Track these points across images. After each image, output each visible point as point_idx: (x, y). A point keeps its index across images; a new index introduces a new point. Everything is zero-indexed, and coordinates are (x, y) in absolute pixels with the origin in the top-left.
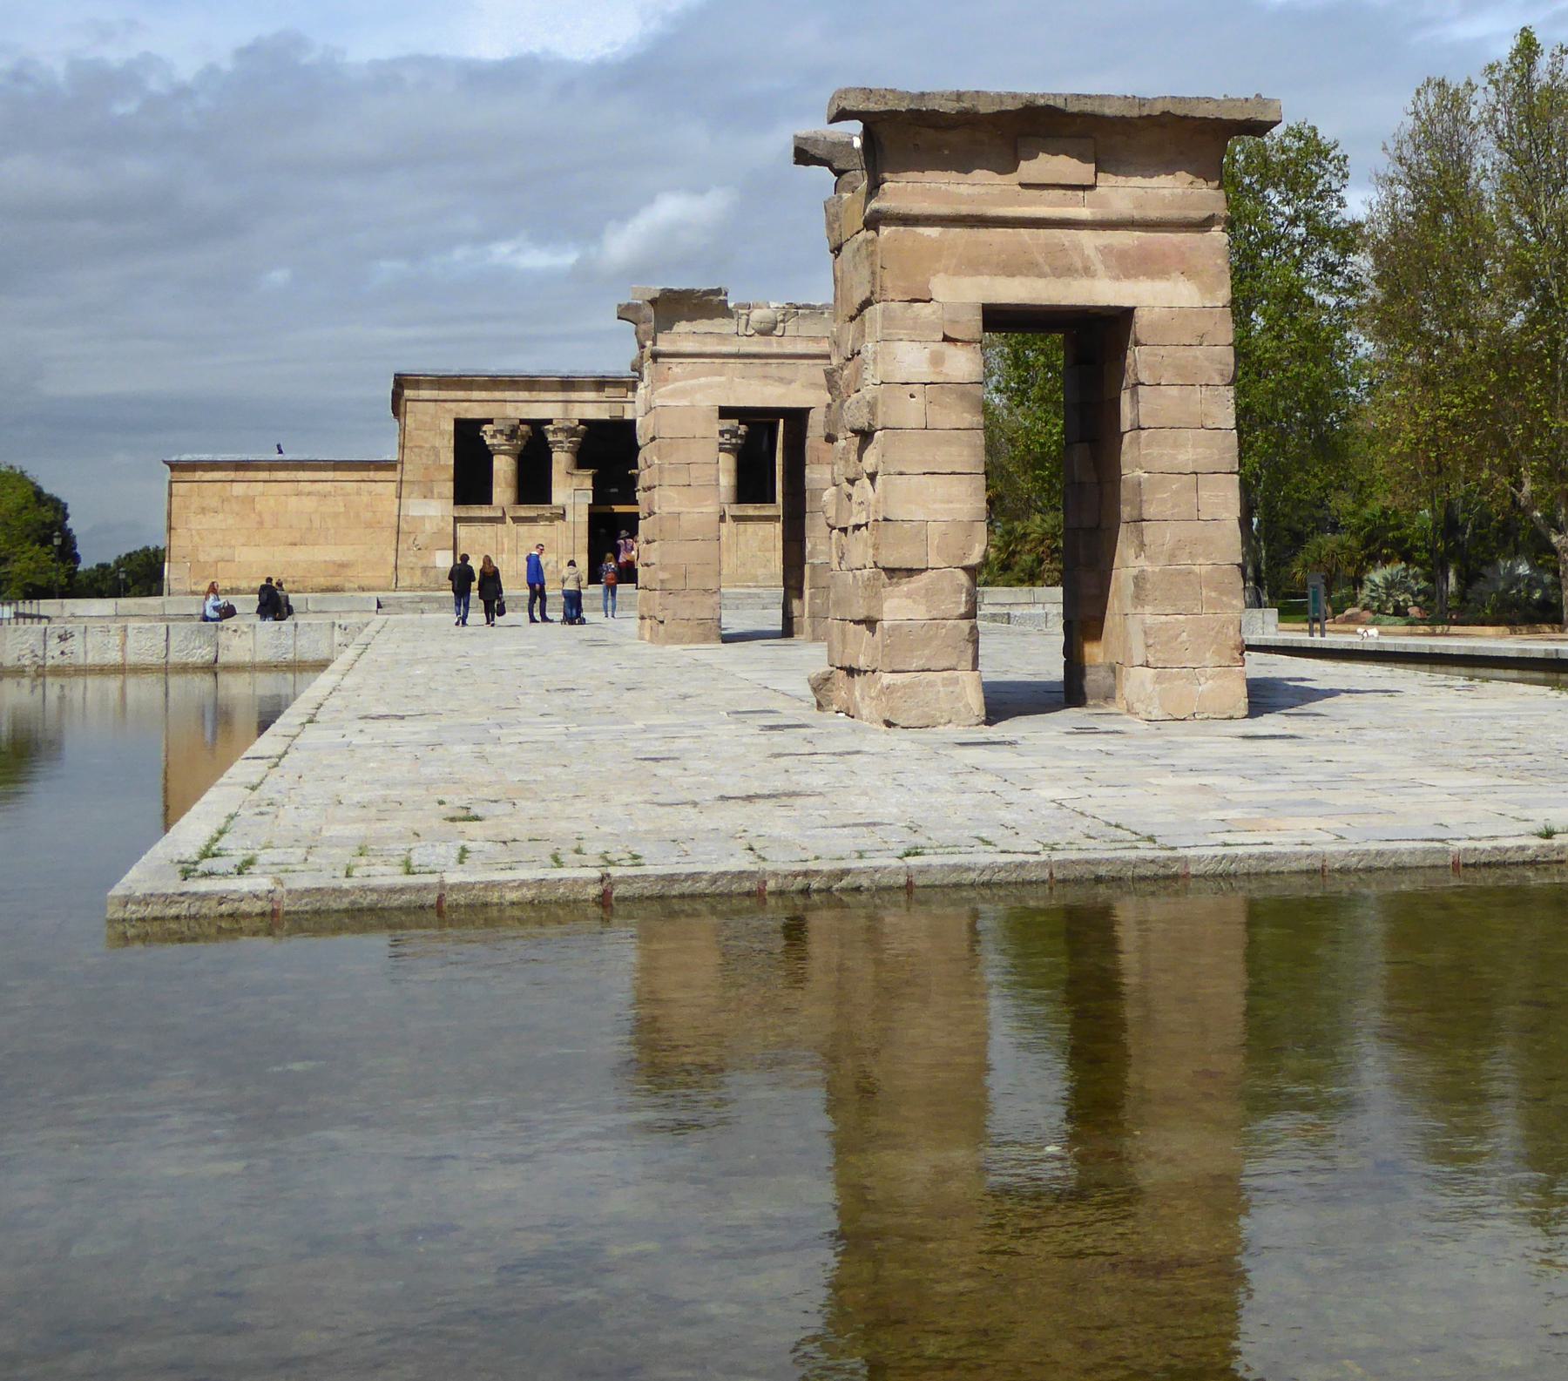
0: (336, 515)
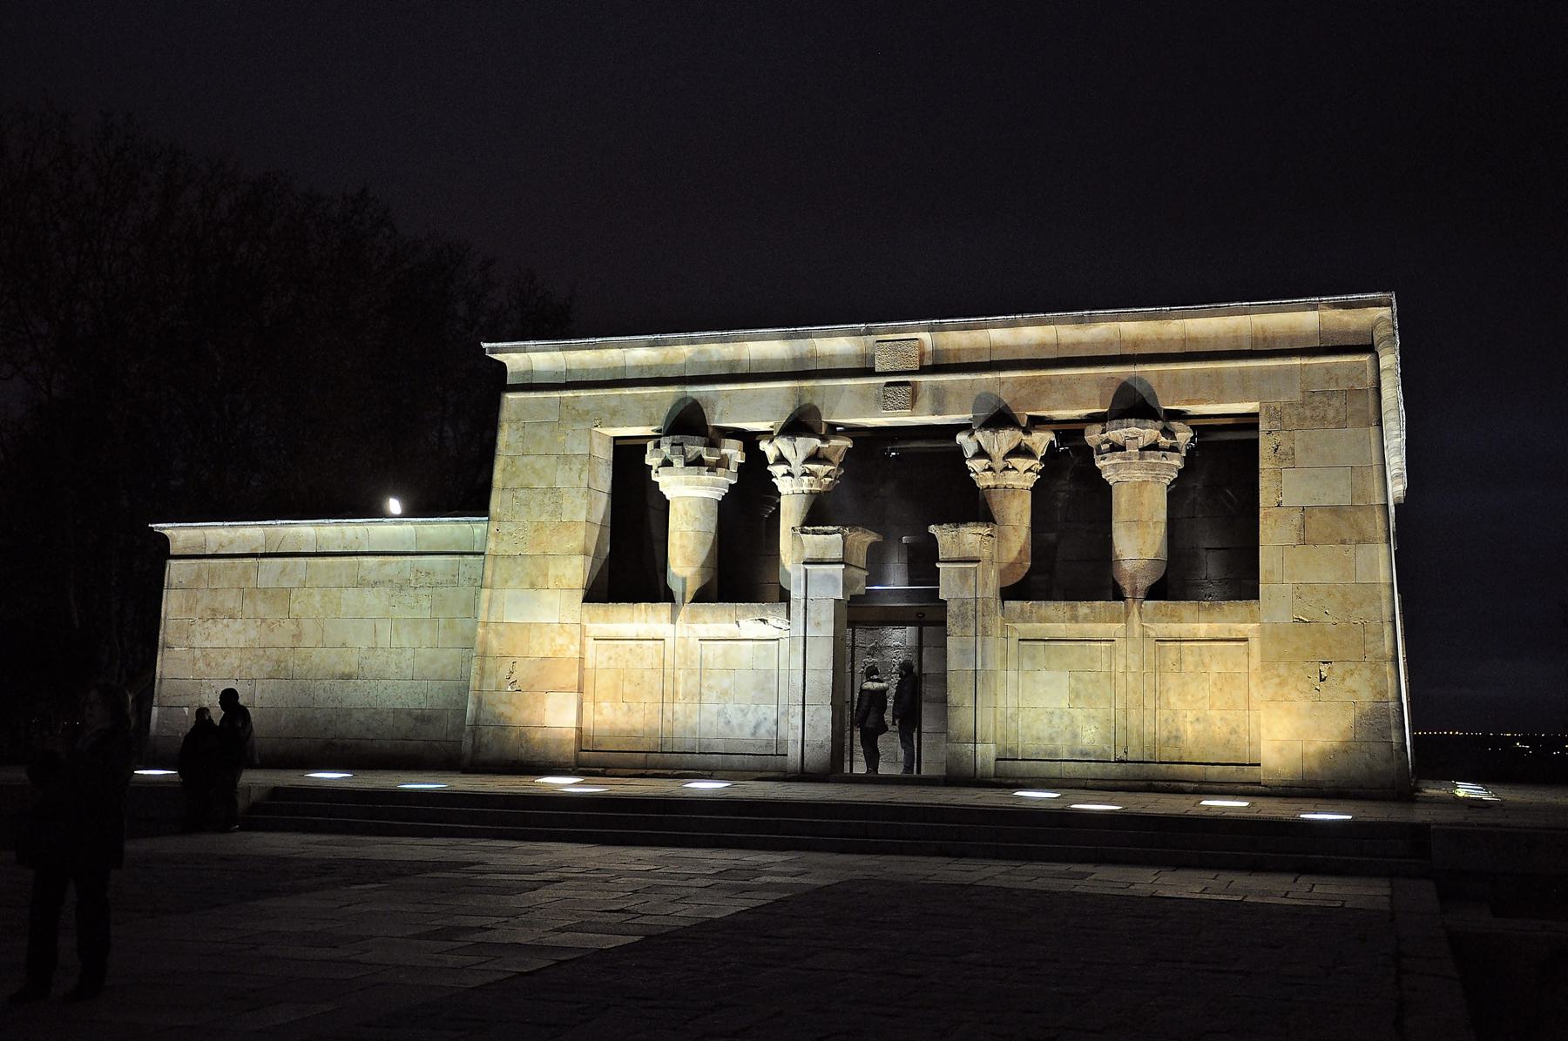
0: (417, 623)
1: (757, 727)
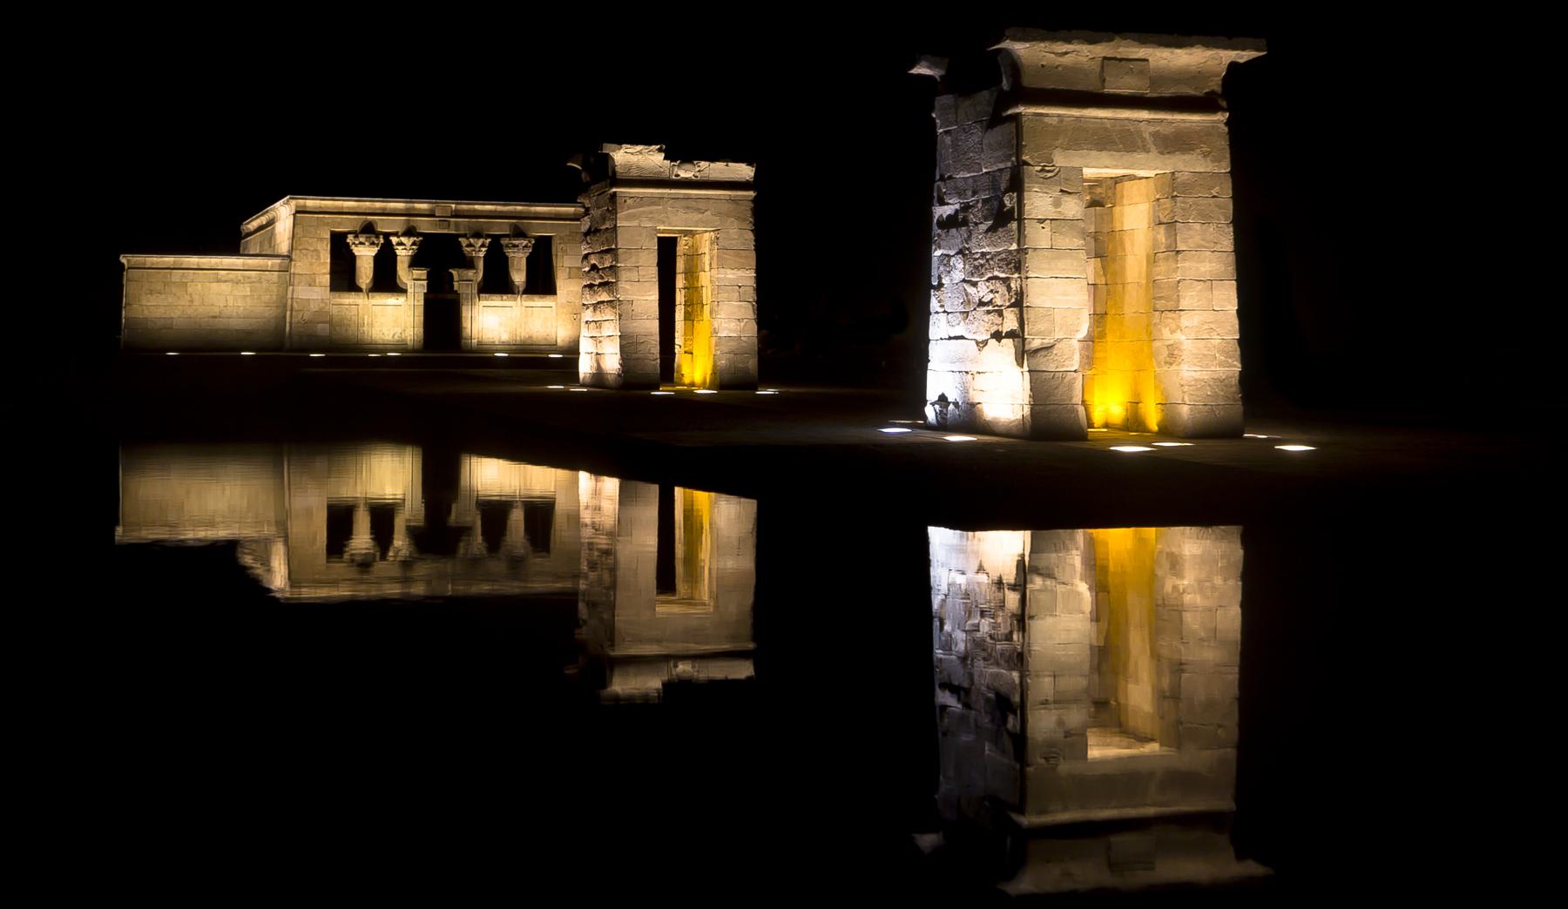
0: (245, 297)
1: (394, 335)
